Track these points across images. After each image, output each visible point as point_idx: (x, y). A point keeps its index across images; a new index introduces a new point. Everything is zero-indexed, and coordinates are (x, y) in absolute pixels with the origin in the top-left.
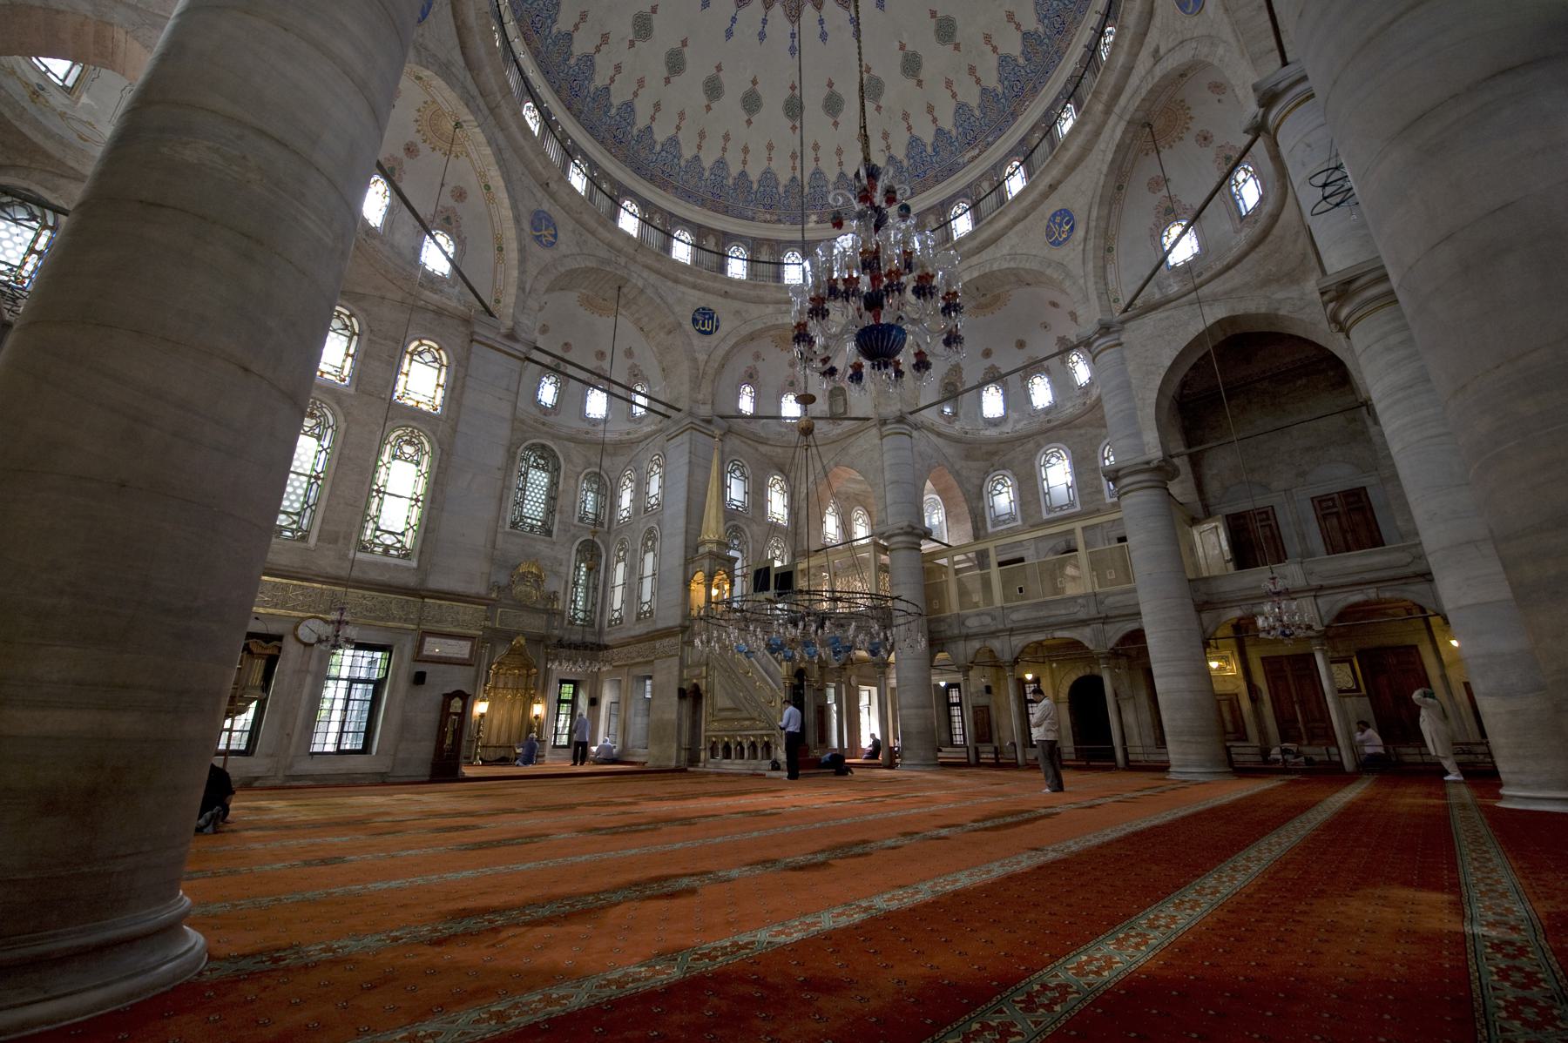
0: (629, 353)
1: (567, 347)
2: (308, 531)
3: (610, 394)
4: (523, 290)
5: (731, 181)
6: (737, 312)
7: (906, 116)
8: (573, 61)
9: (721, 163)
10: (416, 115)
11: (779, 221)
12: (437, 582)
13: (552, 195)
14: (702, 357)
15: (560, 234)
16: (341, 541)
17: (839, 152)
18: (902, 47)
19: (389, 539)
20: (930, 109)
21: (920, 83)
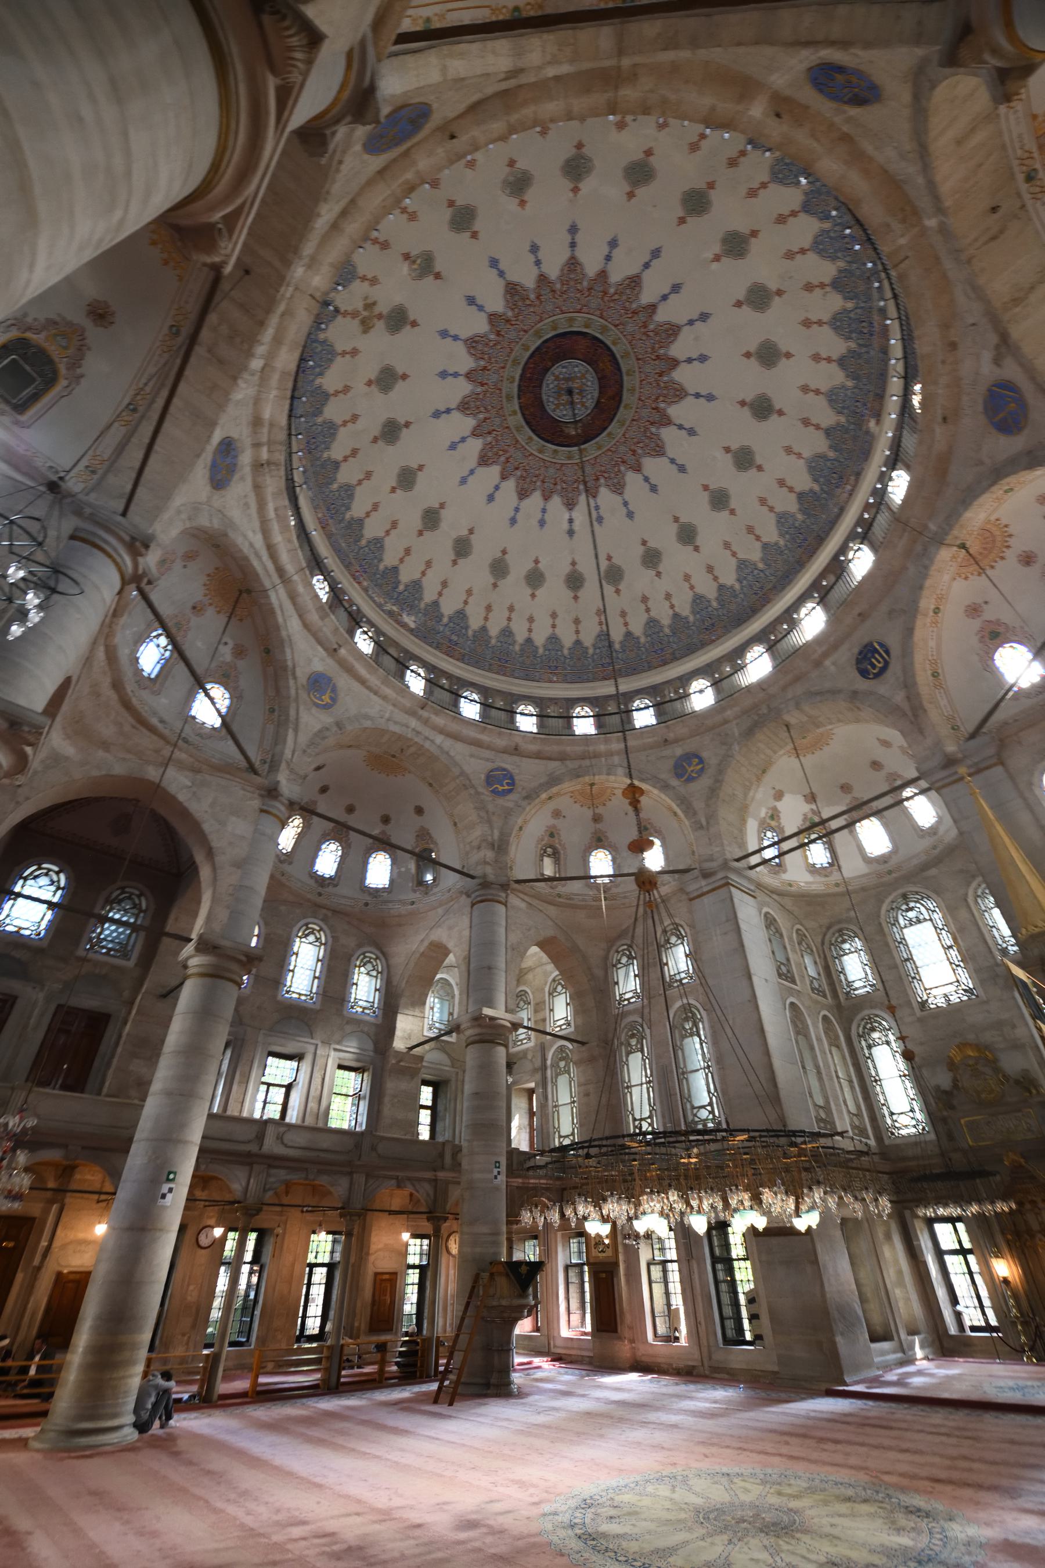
0: (886, 744)
1: (846, 788)
4: (701, 827)
5: (800, 517)
6: (891, 613)
7: (790, 255)
8: (643, 640)
9: (782, 519)
10: (577, 806)
11: (858, 475)
13: (676, 741)
14: (899, 697)
15: (705, 755)
17: (816, 358)
18: (717, 258)
20: (781, 219)
21: (754, 233)
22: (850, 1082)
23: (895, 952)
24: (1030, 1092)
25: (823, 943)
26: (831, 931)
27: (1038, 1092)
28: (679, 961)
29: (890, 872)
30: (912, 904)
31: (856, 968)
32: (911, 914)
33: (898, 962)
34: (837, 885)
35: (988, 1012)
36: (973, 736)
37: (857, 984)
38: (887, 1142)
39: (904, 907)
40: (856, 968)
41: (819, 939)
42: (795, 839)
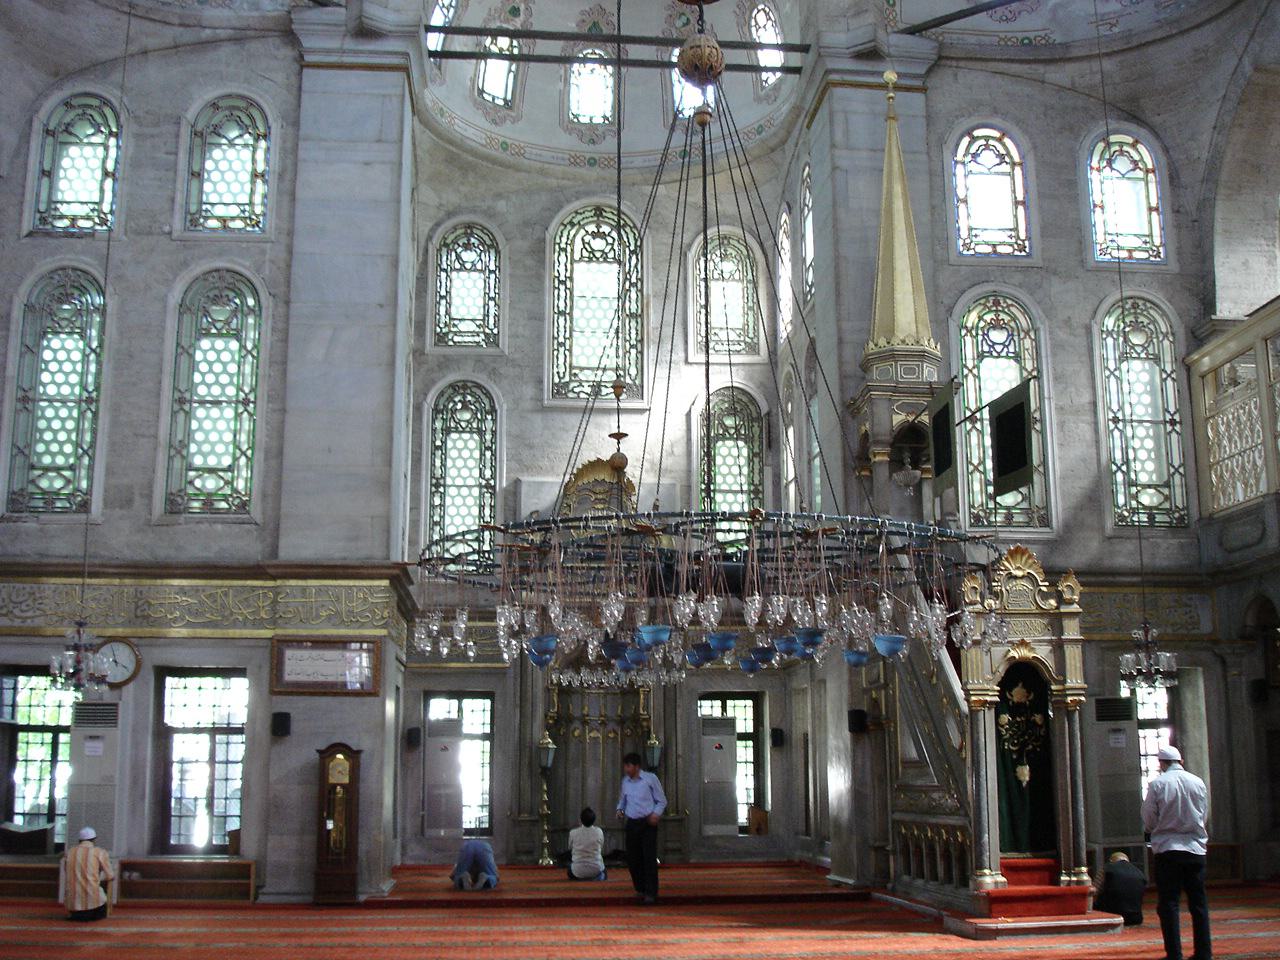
2: (89, 492)
3: (619, 62)
12: (296, 547)
16: (138, 501)
19: (211, 483)
23: (547, 299)
25: (430, 238)
26: (449, 224)
28: (232, 178)
29: (592, 162)
30: (605, 229)
31: (467, 295)
32: (598, 244)
33: (548, 312)
34: (505, 146)
36: (913, 31)
37: (463, 327)
39: (592, 228)
40: (467, 295)
41: (425, 227)
42: (561, 43)
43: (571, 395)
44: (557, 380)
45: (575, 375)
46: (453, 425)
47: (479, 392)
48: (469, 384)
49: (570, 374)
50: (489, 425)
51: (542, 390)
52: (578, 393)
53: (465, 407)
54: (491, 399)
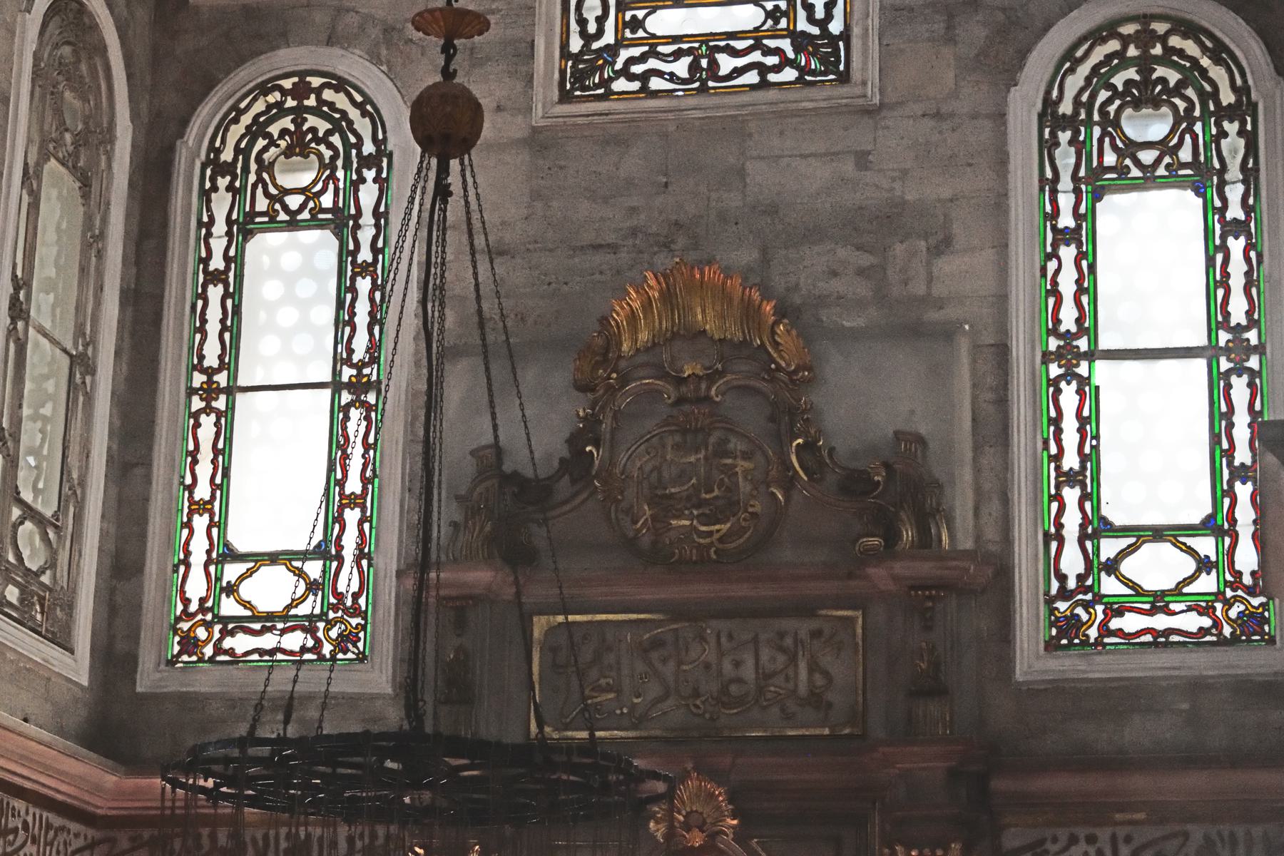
22: (82, 363)
24: (892, 537)
27: (925, 540)
35: (862, 160)
38: (148, 678)
43: (621, 85)
44: (576, 44)
45: (636, 24)
46: (262, 204)
47: (341, 101)
48: (316, 82)
49: (621, 26)
50: (368, 195)
51: (530, 79)
52: (645, 77)
53: (299, 145)
54: (376, 119)
